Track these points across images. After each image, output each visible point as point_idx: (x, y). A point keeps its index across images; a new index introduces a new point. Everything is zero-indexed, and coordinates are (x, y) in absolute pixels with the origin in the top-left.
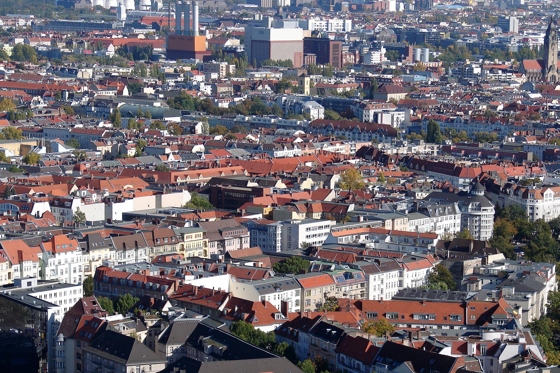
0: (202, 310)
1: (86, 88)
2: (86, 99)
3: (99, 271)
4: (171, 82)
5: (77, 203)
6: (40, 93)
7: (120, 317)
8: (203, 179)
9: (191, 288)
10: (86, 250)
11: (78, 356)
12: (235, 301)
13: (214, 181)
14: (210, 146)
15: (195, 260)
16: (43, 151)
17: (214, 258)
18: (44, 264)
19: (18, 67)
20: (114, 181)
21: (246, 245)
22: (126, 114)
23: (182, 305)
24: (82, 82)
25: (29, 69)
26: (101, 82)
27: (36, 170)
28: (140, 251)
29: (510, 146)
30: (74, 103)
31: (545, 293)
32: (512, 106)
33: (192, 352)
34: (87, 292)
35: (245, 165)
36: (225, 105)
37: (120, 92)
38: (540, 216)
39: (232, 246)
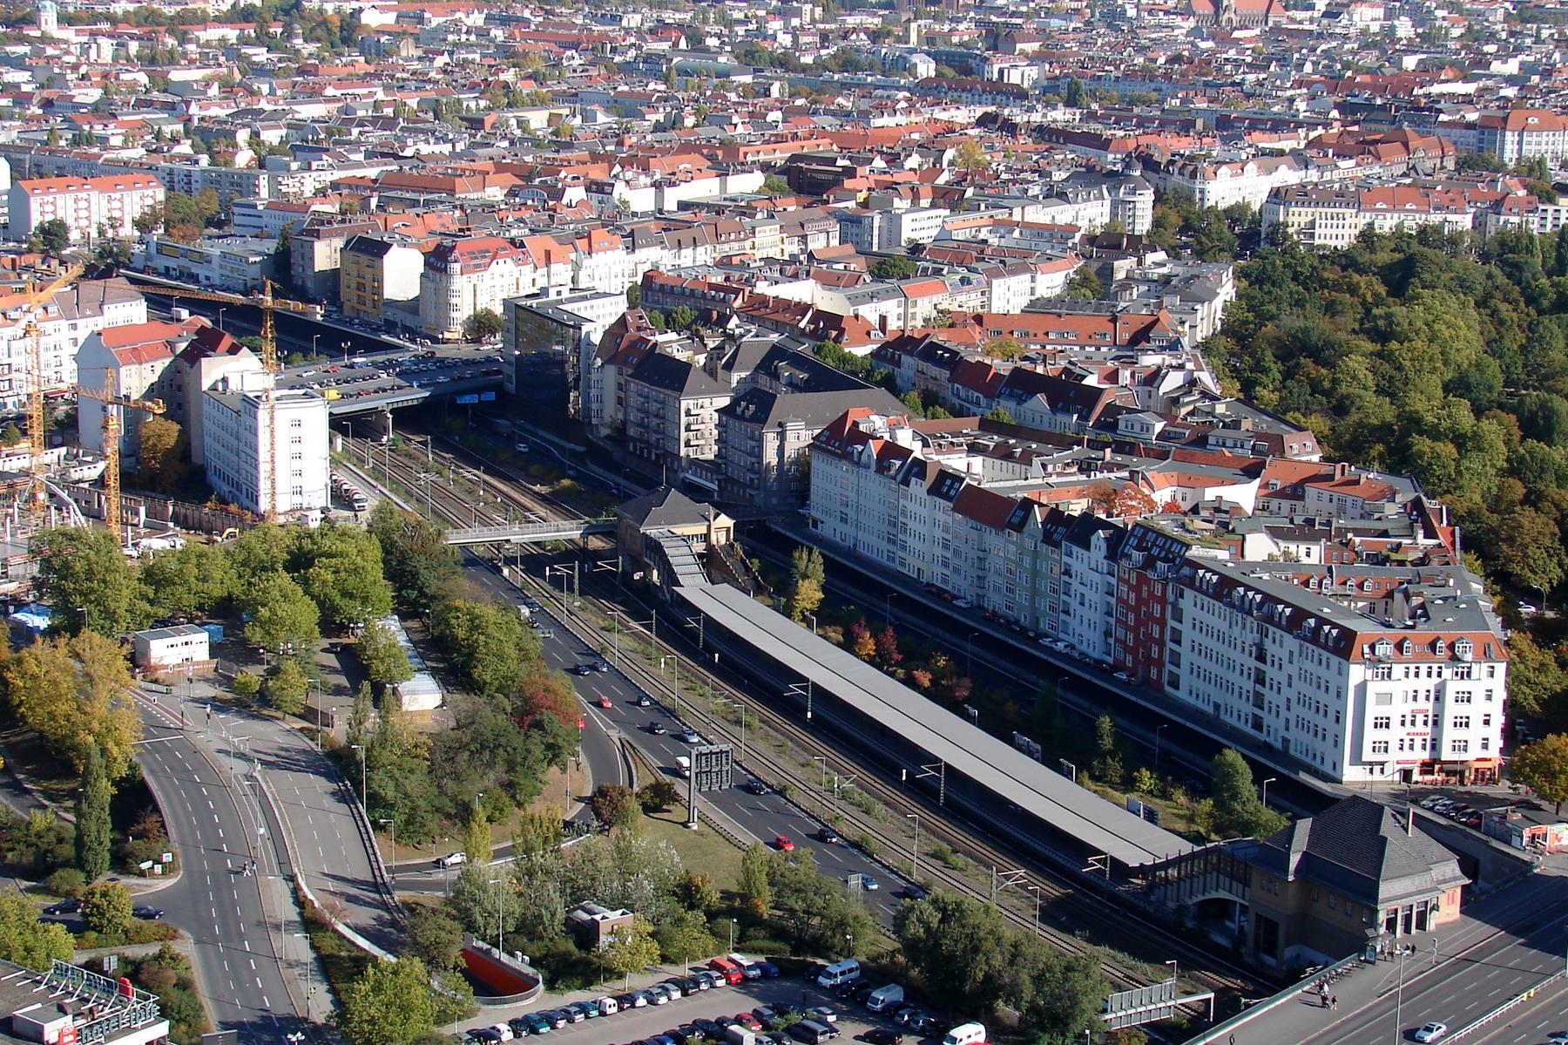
0: (778, 327)
1: (633, 40)
2: (632, 53)
3: (647, 277)
4: (740, 30)
5: (620, 189)
6: (575, 47)
7: (672, 336)
8: (780, 157)
9: (763, 300)
10: (632, 248)
11: (620, 387)
12: (820, 315)
13: (794, 158)
14: (789, 113)
15: (769, 261)
16: (578, 121)
17: (794, 259)
18: (577, 267)
19: (547, 12)
20: (668, 159)
21: (835, 242)
22: (684, 72)
23: (752, 320)
24: (628, 31)
25: (561, 14)
26: (651, 31)
27: (569, 146)
28: (700, 250)
29: (1173, 111)
30: (617, 59)
31: (1218, 303)
32: (1175, 59)
33: (764, 382)
34: (632, 305)
35: (834, 137)
36: (808, 59)
37: (676, 44)
38: (1211, 203)
39: (817, 243)
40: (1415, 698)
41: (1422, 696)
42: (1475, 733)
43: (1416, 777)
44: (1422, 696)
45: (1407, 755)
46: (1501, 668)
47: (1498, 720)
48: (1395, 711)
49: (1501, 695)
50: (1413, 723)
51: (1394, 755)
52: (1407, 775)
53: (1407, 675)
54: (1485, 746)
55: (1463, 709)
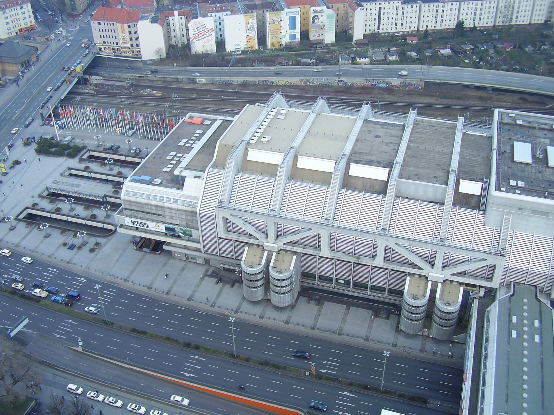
40: (13, 16)
41: (14, 15)
42: (28, 20)
43: (19, 33)
44: (14, 15)
45: (15, 29)
46: (29, 5)
47: (32, 16)
48: (9, 20)
49: (31, 10)
50: (14, 22)
51: (12, 29)
52: (17, 33)
53: (10, 11)
54: (31, 22)
55: (24, 16)
